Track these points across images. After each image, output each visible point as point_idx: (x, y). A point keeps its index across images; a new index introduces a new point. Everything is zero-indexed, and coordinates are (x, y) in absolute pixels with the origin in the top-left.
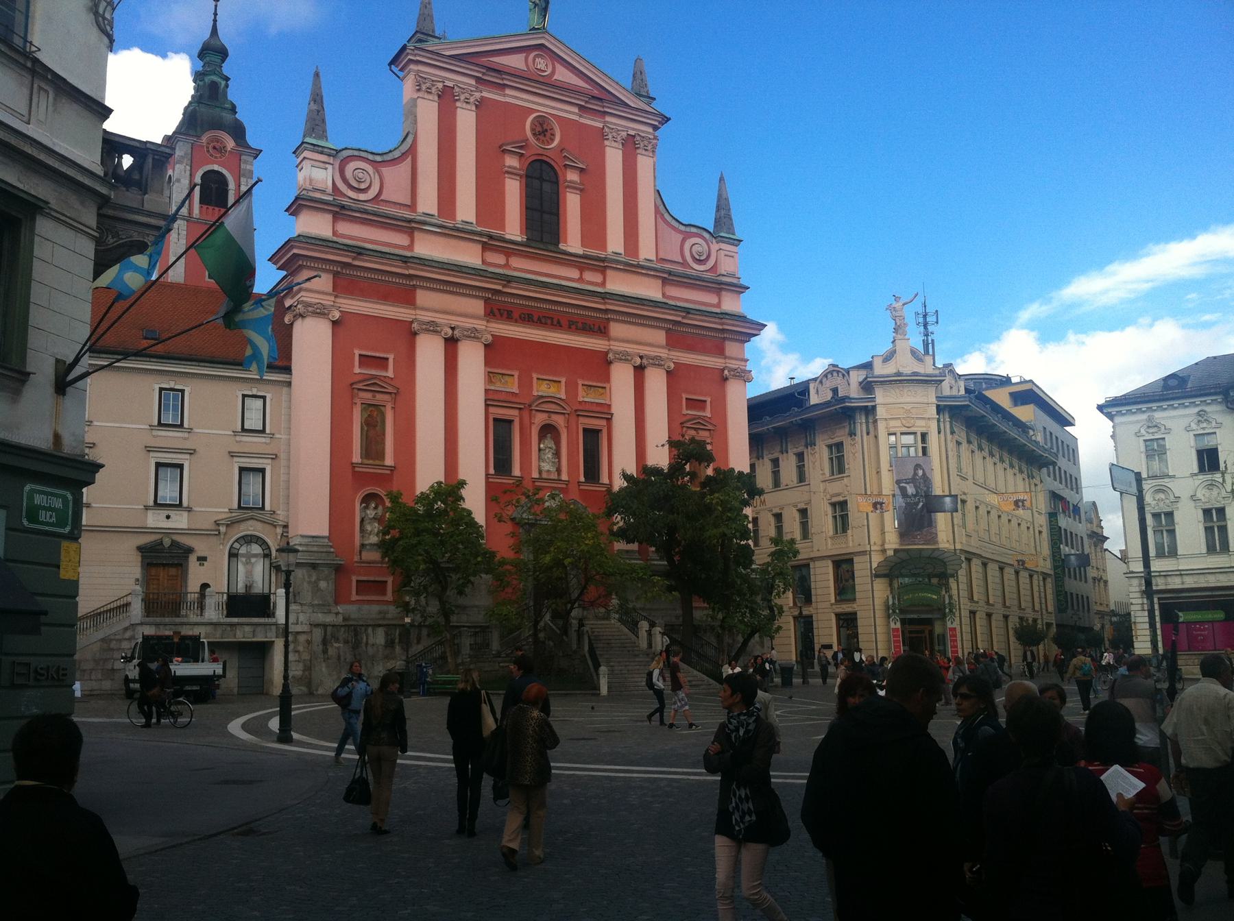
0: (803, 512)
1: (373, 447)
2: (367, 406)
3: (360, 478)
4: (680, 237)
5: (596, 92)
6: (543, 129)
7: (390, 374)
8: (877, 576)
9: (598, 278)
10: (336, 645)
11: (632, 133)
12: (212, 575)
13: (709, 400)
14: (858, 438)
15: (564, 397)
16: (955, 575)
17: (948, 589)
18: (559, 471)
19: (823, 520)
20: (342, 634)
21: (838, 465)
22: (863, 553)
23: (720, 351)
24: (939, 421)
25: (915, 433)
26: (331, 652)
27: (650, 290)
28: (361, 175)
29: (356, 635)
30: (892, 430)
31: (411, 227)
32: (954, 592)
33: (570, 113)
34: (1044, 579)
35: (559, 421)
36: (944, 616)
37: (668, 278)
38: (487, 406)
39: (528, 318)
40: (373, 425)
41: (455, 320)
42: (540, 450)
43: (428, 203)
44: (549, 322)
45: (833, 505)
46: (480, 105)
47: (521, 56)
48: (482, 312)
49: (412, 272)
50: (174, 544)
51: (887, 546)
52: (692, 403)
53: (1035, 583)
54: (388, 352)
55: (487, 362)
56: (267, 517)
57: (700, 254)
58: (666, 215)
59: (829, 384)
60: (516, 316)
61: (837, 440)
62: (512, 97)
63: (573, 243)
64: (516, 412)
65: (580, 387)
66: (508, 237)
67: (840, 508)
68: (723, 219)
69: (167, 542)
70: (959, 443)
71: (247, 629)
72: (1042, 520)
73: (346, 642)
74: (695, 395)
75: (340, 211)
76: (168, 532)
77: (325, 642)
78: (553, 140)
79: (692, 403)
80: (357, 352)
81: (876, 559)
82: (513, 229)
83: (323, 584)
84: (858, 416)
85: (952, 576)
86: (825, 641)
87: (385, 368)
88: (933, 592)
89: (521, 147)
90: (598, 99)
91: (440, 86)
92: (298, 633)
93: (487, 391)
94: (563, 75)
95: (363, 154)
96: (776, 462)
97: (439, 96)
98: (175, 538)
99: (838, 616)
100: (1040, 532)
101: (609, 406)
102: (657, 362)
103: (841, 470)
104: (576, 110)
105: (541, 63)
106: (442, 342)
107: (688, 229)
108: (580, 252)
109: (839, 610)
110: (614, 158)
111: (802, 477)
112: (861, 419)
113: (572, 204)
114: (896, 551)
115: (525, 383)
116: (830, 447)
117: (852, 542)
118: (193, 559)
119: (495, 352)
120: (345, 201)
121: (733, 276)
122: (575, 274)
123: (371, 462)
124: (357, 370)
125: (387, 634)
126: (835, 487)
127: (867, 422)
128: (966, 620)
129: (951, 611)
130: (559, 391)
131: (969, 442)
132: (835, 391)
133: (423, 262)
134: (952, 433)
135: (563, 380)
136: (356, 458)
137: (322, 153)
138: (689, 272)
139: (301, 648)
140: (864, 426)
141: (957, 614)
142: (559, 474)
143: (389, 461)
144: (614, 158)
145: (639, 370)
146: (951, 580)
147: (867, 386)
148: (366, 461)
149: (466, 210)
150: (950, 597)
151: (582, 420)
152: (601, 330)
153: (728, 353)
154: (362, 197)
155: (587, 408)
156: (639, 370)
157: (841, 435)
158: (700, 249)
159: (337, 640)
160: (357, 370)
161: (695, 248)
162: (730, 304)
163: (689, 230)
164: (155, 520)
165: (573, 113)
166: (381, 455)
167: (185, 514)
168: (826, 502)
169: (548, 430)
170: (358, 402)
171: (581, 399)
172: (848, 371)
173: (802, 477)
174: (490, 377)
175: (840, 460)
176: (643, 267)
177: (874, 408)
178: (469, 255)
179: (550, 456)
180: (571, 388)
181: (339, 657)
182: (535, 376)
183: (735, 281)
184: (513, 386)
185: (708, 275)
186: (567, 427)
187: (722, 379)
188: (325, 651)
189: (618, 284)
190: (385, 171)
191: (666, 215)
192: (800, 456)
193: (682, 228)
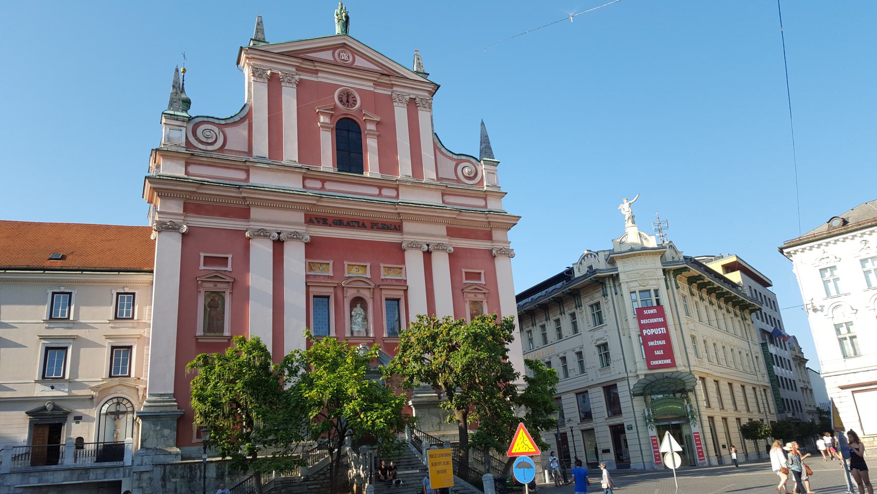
0: (579, 354)
2: (209, 294)
3: (201, 346)
4: (454, 163)
6: (347, 98)
7: (229, 268)
8: (635, 395)
9: (393, 193)
10: (174, 480)
11: (413, 97)
12: (86, 431)
13: (483, 272)
14: (609, 297)
15: (369, 277)
16: (693, 390)
17: (689, 401)
18: (367, 331)
19: (592, 358)
20: (180, 472)
21: (599, 319)
22: (622, 379)
23: (488, 236)
24: (666, 280)
25: (649, 290)
26: (169, 486)
27: (434, 199)
28: (208, 133)
29: (191, 471)
30: (633, 290)
32: (694, 403)
33: (368, 86)
34: (765, 390)
35: (366, 295)
36: (688, 421)
38: (307, 287)
39: (339, 223)
40: (214, 305)
41: (280, 228)
42: (351, 316)
43: (261, 148)
44: (356, 225)
45: (599, 346)
46: (300, 84)
47: (331, 52)
48: (303, 221)
49: (244, 195)
50: (56, 408)
51: (638, 373)
52: (469, 276)
53: (758, 393)
55: (307, 256)
56: (133, 384)
57: (469, 173)
58: (443, 149)
59: (586, 264)
60: (329, 222)
61: (596, 301)
62: (323, 78)
65: (382, 269)
67: (603, 346)
68: (486, 149)
69: (49, 406)
70: (684, 297)
71: (100, 471)
72: (757, 350)
73: (183, 477)
74: (474, 271)
75: (190, 157)
76: (54, 400)
77: (164, 479)
78: (355, 104)
79: (469, 276)
80: (202, 255)
81: (633, 382)
82: (327, 162)
83: (166, 432)
84: (607, 282)
85: (691, 391)
86: (605, 447)
87: (226, 265)
88: (678, 404)
89: (332, 110)
90: (387, 75)
91: (269, 72)
92: (142, 472)
93: (307, 276)
94: (360, 62)
95: (210, 120)
96: (558, 321)
97: (269, 80)
98: (57, 403)
99: (611, 427)
100: (757, 357)
101: (406, 281)
102: (440, 247)
103: (601, 322)
104: (371, 84)
105: (344, 56)
106: (271, 244)
107: (459, 157)
109: (612, 423)
110: (401, 114)
111: (575, 330)
112: (609, 284)
113: (371, 144)
114: (646, 375)
116: (591, 306)
117: (615, 371)
118: (70, 418)
119: (313, 248)
120: (196, 152)
121: (495, 186)
122: (376, 191)
123: (212, 334)
124: (202, 267)
125: (218, 468)
126: (598, 334)
127: (615, 286)
128: (706, 423)
129: (693, 417)
130: (365, 272)
131: (692, 294)
132: (590, 267)
133: (256, 188)
134: (678, 287)
135: (368, 265)
136: (200, 332)
137: (177, 120)
139: (144, 485)
140: (613, 289)
141: (698, 419)
142: (367, 333)
143: (227, 333)
144: (401, 114)
145: (428, 254)
146: (690, 394)
147: (611, 261)
148: (208, 334)
149: (291, 152)
150: (691, 406)
152: (397, 228)
153: (494, 238)
154: (210, 148)
155: (388, 282)
156: (428, 254)
157: (598, 297)
159: (175, 476)
161: (466, 170)
162: (493, 205)
163: (460, 158)
164: (43, 391)
165: (369, 86)
167: (67, 384)
168: (593, 345)
169: (358, 301)
170: (202, 291)
172: (597, 253)
173: (575, 330)
174: (310, 266)
175: (599, 314)
176: (426, 184)
177: (618, 275)
178: (294, 183)
179: (360, 320)
180: (375, 270)
181: (176, 489)
182: (346, 263)
183: (496, 190)
186: (373, 298)
187: (491, 256)
188: (164, 486)
189: (407, 196)
190: (227, 130)
191: (443, 149)
192: (573, 315)
193: (455, 157)
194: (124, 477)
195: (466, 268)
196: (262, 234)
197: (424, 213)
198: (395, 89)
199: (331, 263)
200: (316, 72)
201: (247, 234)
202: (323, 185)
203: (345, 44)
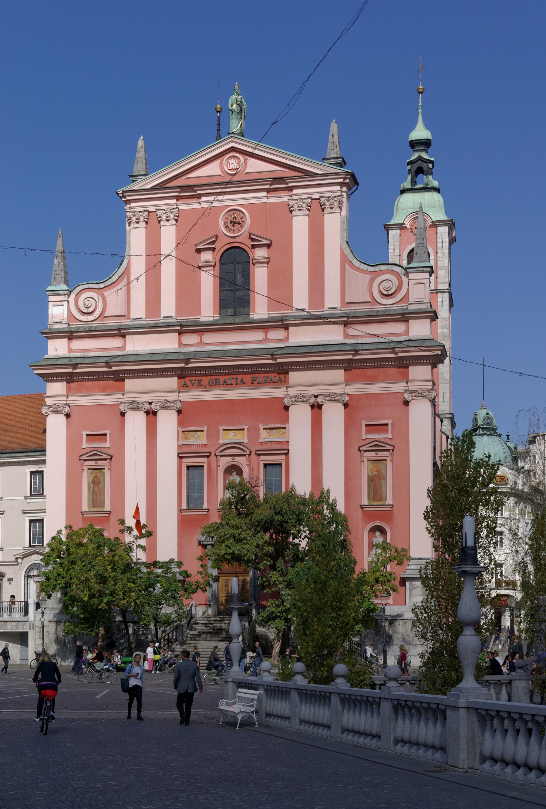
1: (97, 498)
5: (285, 172)
7: (108, 445)
27: (332, 335)
28: (87, 303)
31: (121, 333)
37: (347, 321)
38: (180, 458)
44: (234, 382)
54: (105, 429)
63: (260, 310)
64: (205, 459)
66: (202, 319)
80: (84, 433)
93: (180, 446)
105: (233, 164)
107: (378, 268)
108: (265, 316)
113: (260, 277)
115: (213, 435)
118: (5, 579)
122: (259, 335)
135: (246, 427)
136: (85, 507)
138: (377, 307)
151: (262, 458)
154: (90, 318)
158: (386, 284)
160: (85, 445)
166: (103, 504)
171: (261, 440)
178: (167, 343)
180: (254, 432)
182: (221, 428)
184: (202, 439)
185: (401, 307)
190: (106, 293)
193: (371, 269)
194: (30, 629)
195: (367, 419)
196: (135, 406)
197: (316, 359)
198: (295, 191)
199: (205, 429)
200: (199, 197)
201: (122, 408)
202: (201, 339)
203: (233, 147)
